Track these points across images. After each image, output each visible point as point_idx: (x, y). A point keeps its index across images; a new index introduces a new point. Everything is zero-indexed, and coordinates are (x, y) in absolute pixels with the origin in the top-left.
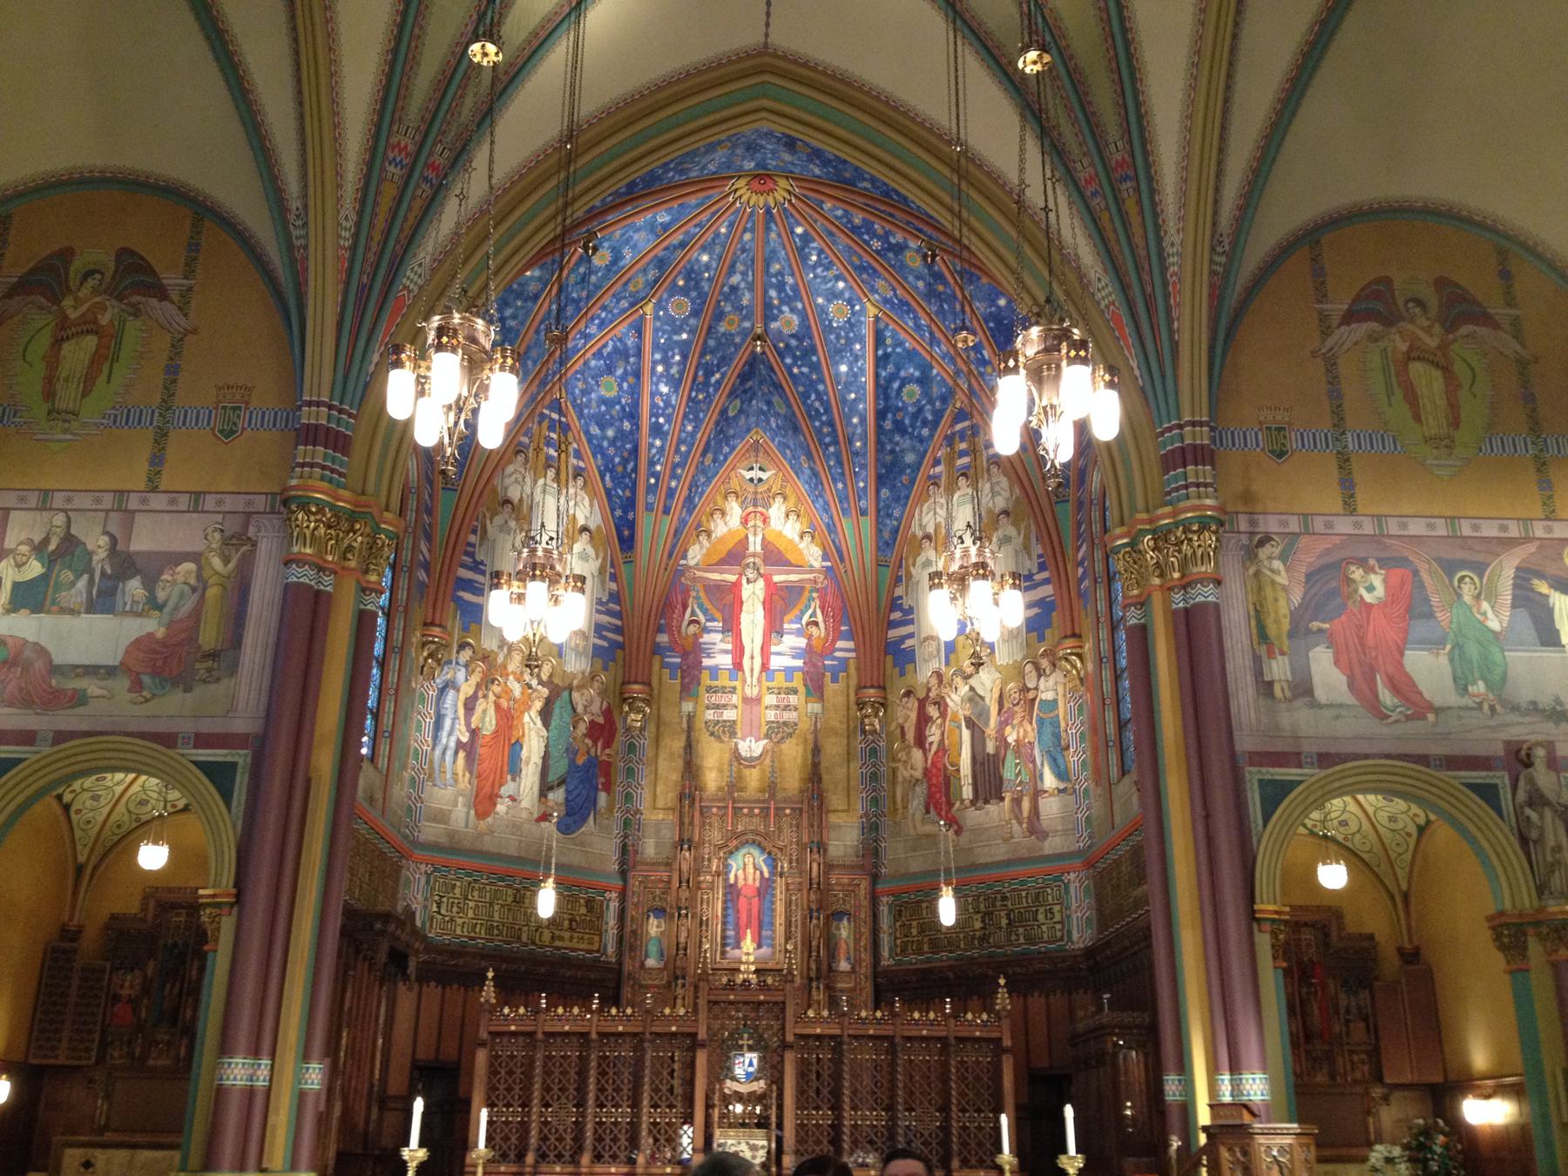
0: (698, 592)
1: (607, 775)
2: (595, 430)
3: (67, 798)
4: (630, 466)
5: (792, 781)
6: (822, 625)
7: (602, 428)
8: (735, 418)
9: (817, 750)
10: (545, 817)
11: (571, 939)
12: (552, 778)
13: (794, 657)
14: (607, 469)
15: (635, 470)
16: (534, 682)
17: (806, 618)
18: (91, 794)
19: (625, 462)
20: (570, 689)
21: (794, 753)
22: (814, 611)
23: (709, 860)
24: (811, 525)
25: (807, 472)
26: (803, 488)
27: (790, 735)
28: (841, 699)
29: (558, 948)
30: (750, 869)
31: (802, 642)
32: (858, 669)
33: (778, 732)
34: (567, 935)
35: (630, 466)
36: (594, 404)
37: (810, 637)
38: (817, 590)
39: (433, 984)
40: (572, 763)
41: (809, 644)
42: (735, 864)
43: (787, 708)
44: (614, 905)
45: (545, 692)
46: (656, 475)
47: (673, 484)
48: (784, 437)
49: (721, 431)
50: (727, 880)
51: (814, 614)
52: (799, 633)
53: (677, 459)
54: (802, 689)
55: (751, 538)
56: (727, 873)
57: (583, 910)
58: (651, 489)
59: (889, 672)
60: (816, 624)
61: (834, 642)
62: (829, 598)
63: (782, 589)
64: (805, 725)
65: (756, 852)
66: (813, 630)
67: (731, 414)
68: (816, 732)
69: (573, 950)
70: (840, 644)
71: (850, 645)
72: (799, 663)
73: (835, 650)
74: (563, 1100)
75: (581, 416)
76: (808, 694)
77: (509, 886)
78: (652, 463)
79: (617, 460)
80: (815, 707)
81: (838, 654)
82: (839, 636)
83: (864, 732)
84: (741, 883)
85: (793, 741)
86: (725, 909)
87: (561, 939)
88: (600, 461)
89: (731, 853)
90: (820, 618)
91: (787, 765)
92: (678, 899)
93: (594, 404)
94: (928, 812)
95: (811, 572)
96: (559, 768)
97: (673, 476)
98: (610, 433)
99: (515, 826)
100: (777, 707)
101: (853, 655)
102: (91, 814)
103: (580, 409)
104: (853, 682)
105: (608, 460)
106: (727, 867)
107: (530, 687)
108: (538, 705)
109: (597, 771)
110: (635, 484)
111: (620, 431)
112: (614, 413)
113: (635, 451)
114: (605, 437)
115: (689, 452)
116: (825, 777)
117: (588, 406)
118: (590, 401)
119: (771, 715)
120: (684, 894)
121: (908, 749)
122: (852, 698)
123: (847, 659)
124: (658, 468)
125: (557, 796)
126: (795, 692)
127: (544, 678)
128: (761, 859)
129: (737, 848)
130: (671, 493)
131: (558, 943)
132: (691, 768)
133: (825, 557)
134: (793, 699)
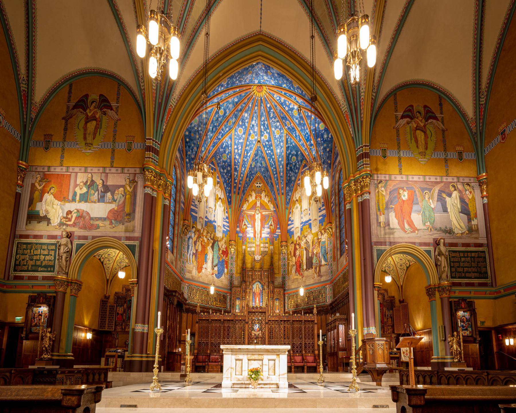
0: (245, 216)
1: (227, 265)
2: (222, 170)
3: (102, 260)
4: (230, 181)
5: (266, 266)
6: (273, 226)
7: (223, 170)
8: (254, 168)
9: (272, 258)
10: (213, 274)
11: (220, 304)
12: (214, 264)
13: (267, 234)
14: (225, 181)
15: (231, 182)
16: (210, 239)
17: (270, 224)
18: (107, 259)
19: (229, 179)
20: (218, 241)
21: (267, 258)
22: (271, 222)
23: (249, 286)
24: (271, 199)
25: (270, 183)
26: (269, 188)
27: (266, 254)
28: (277, 245)
29: (217, 307)
30: (258, 288)
31: (269, 230)
32: (281, 237)
33: (264, 254)
34: (219, 303)
35: (230, 181)
36: (221, 163)
37: (270, 229)
38: (272, 216)
39: (190, 313)
40: (219, 260)
41: (270, 231)
42: (255, 286)
43: (265, 247)
44: (229, 297)
45: (212, 241)
46: (236, 183)
47: (240, 186)
48: (265, 174)
49: (250, 172)
50: (252, 291)
51: (271, 223)
52: (268, 228)
53: (241, 179)
54: (269, 242)
55: (257, 202)
56: (253, 289)
57: (222, 298)
58: (235, 187)
59: (288, 238)
60: (272, 225)
61: (276, 230)
62: (275, 218)
63: (264, 216)
64: (269, 252)
65: (259, 283)
66: (271, 227)
67: (253, 167)
68: (272, 254)
69: (220, 307)
70: (277, 231)
71: (279, 231)
72: (268, 236)
73: (276, 232)
74: (216, 337)
75: (218, 166)
76: (270, 244)
77: (206, 291)
78: (235, 180)
79: (227, 179)
80: (272, 247)
81: (277, 233)
82: (277, 228)
83: (282, 253)
84: (256, 292)
85: (267, 256)
86: (252, 298)
87: (218, 304)
88: (223, 180)
89: (254, 284)
90: (273, 224)
91: (265, 262)
92: (242, 295)
93: (221, 163)
94: (296, 273)
95: (271, 211)
96: (216, 262)
97: (240, 184)
98: (225, 171)
99: (207, 276)
100: (263, 247)
101: (280, 233)
102: (109, 265)
103: (218, 164)
104: (280, 240)
105: (225, 179)
106: (253, 287)
107: (209, 240)
108: (211, 245)
109: (224, 263)
110: (231, 185)
111: (227, 170)
112: (226, 165)
113: (231, 176)
114: (224, 172)
115: (243, 176)
116: (274, 265)
117: (220, 163)
118: (220, 162)
119: (262, 249)
120: (244, 294)
121: (292, 257)
122: (280, 245)
123: (279, 235)
124: (236, 181)
125: (216, 269)
126: (267, 243)
127: (212, 238)
128: (260, 285)
129: (255, 283)
130: (239, 188)
131: (217, 305)
132: (244, 262)
133: (274, 207)
134: (267, 245)
